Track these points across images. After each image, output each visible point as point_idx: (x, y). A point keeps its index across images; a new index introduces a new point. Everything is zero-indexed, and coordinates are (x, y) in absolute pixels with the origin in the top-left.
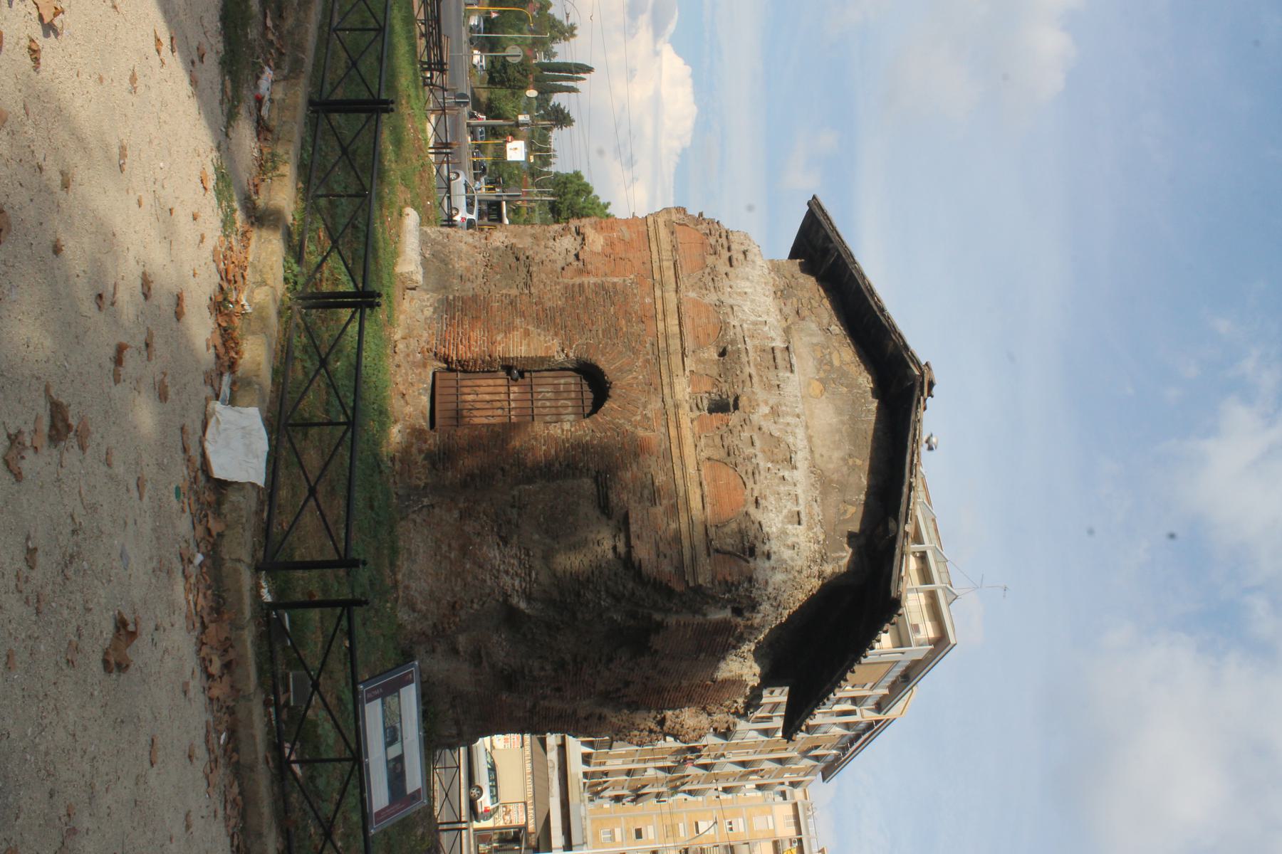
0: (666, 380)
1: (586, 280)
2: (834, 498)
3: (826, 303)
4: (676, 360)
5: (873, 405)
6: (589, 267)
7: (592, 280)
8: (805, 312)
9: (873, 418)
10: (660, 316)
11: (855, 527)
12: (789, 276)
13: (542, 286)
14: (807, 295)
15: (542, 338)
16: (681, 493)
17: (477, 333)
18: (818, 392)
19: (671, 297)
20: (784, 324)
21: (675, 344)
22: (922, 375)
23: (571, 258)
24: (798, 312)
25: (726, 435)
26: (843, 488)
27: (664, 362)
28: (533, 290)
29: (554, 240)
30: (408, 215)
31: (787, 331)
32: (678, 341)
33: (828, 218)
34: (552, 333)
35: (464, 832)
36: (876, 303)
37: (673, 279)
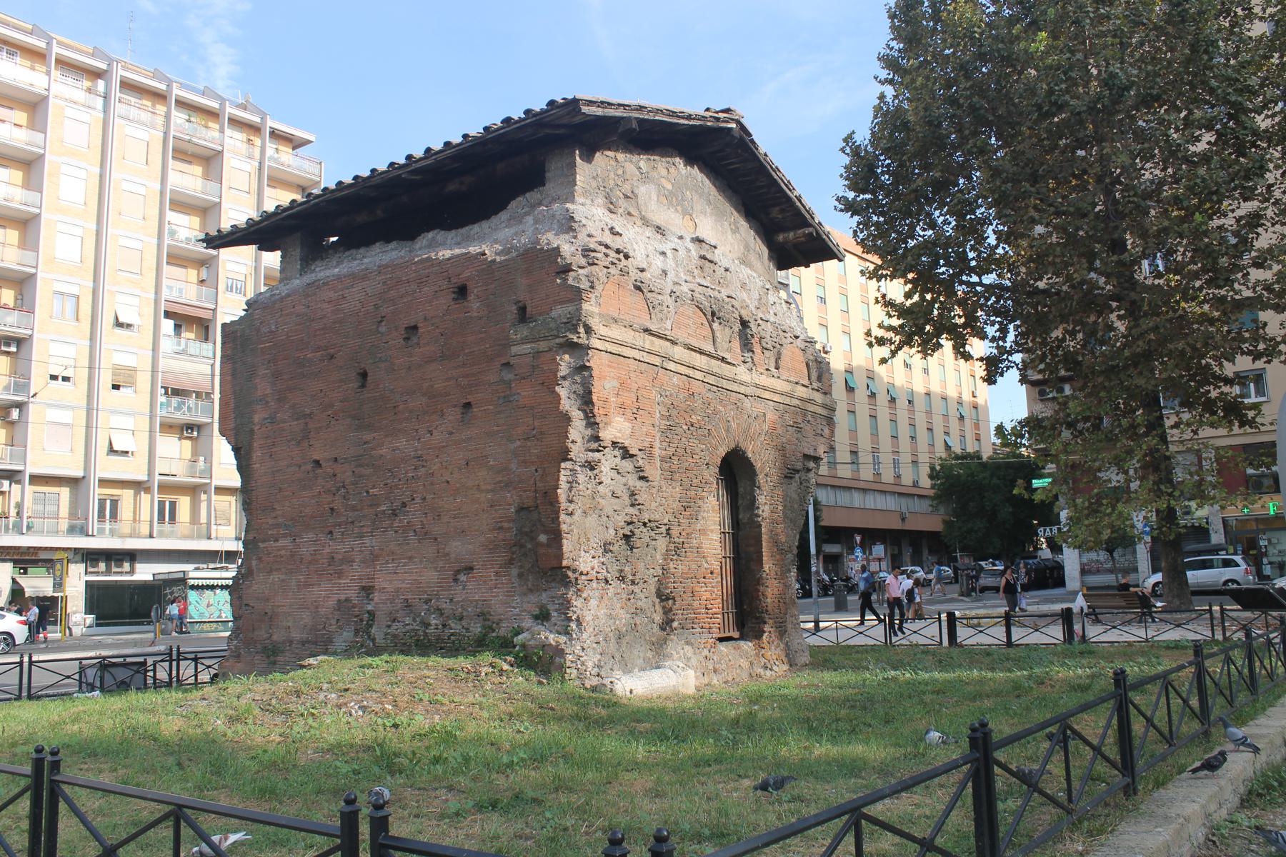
0: (735, 387)
1: (657, 452)
2: (753, 258)
3: (621, 156)
4: (725, 370)
5: (695, 172)
6: (647, 444)
7: (657, 444)
8: (627, 188)
9: (707, 182)
10: (690, 372)
11: (765, 251)
12: (594, 184)
13: (661, 509)
14: (612, 175)
15: (705, 514)
16: (798, 402)
17: (705, 593)
18: (691, 223)
19: (678, 352)
20: (639, 223)
21: (716, 366)
22: (738, 122)
23: (627, 465)
24: (626, 197)
25: (764, 345)
26: (747, 247)
27: (724, 384)
28: (666, 521)
29: (600, 483)
30: (631, 692)
31: (646, 222)
32: (713, 361)
33: (602, 102)
34: (700, 503)
35: (35, 658)
36: (683, 118)
37: (662, 342)
